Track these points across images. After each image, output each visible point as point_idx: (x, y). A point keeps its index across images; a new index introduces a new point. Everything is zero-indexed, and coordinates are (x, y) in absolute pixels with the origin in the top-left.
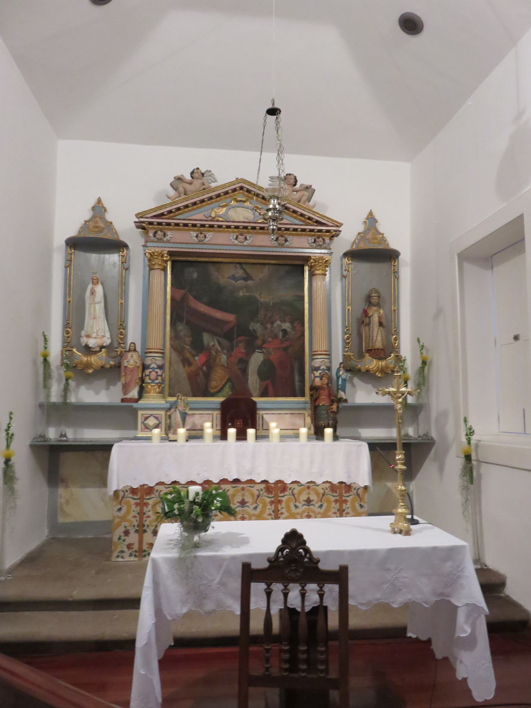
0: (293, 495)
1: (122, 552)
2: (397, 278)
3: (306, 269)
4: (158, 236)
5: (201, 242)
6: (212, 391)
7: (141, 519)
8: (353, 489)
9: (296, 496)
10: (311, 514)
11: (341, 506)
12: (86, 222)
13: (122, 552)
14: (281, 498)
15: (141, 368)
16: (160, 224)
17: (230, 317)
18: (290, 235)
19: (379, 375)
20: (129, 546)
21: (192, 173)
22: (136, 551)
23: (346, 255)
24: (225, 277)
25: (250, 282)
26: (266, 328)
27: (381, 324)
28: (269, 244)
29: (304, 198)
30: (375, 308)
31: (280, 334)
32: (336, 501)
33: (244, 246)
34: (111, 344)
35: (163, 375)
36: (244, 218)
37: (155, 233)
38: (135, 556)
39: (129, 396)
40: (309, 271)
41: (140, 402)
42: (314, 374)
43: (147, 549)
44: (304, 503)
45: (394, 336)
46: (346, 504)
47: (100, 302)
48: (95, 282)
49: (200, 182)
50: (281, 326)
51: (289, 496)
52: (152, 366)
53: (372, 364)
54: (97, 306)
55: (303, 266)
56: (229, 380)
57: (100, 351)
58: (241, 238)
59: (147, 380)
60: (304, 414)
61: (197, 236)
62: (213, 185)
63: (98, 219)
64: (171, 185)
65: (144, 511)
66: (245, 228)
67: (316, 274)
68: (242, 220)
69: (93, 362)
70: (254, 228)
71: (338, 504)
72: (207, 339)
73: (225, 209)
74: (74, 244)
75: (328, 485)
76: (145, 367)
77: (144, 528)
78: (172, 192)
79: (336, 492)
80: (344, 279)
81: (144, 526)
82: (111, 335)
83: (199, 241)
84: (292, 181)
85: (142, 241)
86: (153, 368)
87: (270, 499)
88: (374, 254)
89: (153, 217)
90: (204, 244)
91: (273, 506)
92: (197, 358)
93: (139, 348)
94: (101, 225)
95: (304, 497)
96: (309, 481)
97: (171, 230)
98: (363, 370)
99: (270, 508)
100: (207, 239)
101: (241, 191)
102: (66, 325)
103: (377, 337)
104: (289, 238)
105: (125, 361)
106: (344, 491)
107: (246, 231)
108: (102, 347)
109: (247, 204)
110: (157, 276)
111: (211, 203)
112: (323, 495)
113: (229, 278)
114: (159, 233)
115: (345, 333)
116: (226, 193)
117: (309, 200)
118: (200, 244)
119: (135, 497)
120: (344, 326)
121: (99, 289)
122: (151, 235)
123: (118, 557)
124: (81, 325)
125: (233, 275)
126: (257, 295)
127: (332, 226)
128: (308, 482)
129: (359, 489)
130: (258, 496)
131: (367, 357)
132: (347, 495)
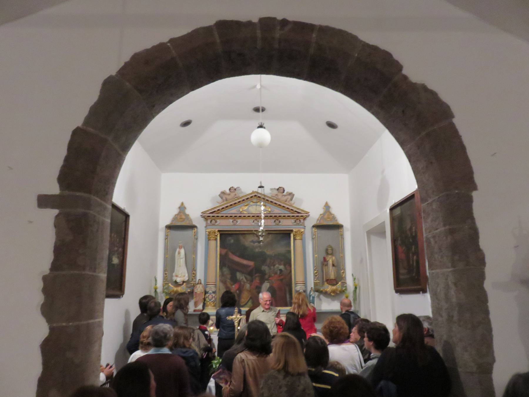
3: (292, 235)
5: (235, 225)
6: (242, 304)
15: (204, 293)
17: (251, 263)
21: (230, 189)
23: (313, 226)
24: (248, 241)
26: (270, 269)
27: (333, 265)
29: (288, 200)
30: (330, 256)
31: (279, 272)
34: (188, 280)
37: (211, 221)
40: (294, 235)
48: (180, 248)
49: (234, 194)
50: (278, 267)
53: (329, 288)
55: (289, 234)
56: (251, 298)
57: (183, 284)
59: (207, 299)
62: (241, 195)
72: (239, 276)
74: (169, 227)
76: (206, 293)
78: (220, 200)
82: (188, 275)
84: (282, 191)
85: (204, 223)
88: (329, 226)
92: (233, 286)
93: (203, 282)
94: (183, 217)
98: (324, 291)
102: (165, 270)
108: (184, 282)
110: (213, 243)
114: (213, 221)
115: (315, 270)
116: (248, 199)
117: (291, 200)
120: (314, 266)
121: (182, 251)
122: (209, 222)
124: (173, 270)
126: (265, 251)
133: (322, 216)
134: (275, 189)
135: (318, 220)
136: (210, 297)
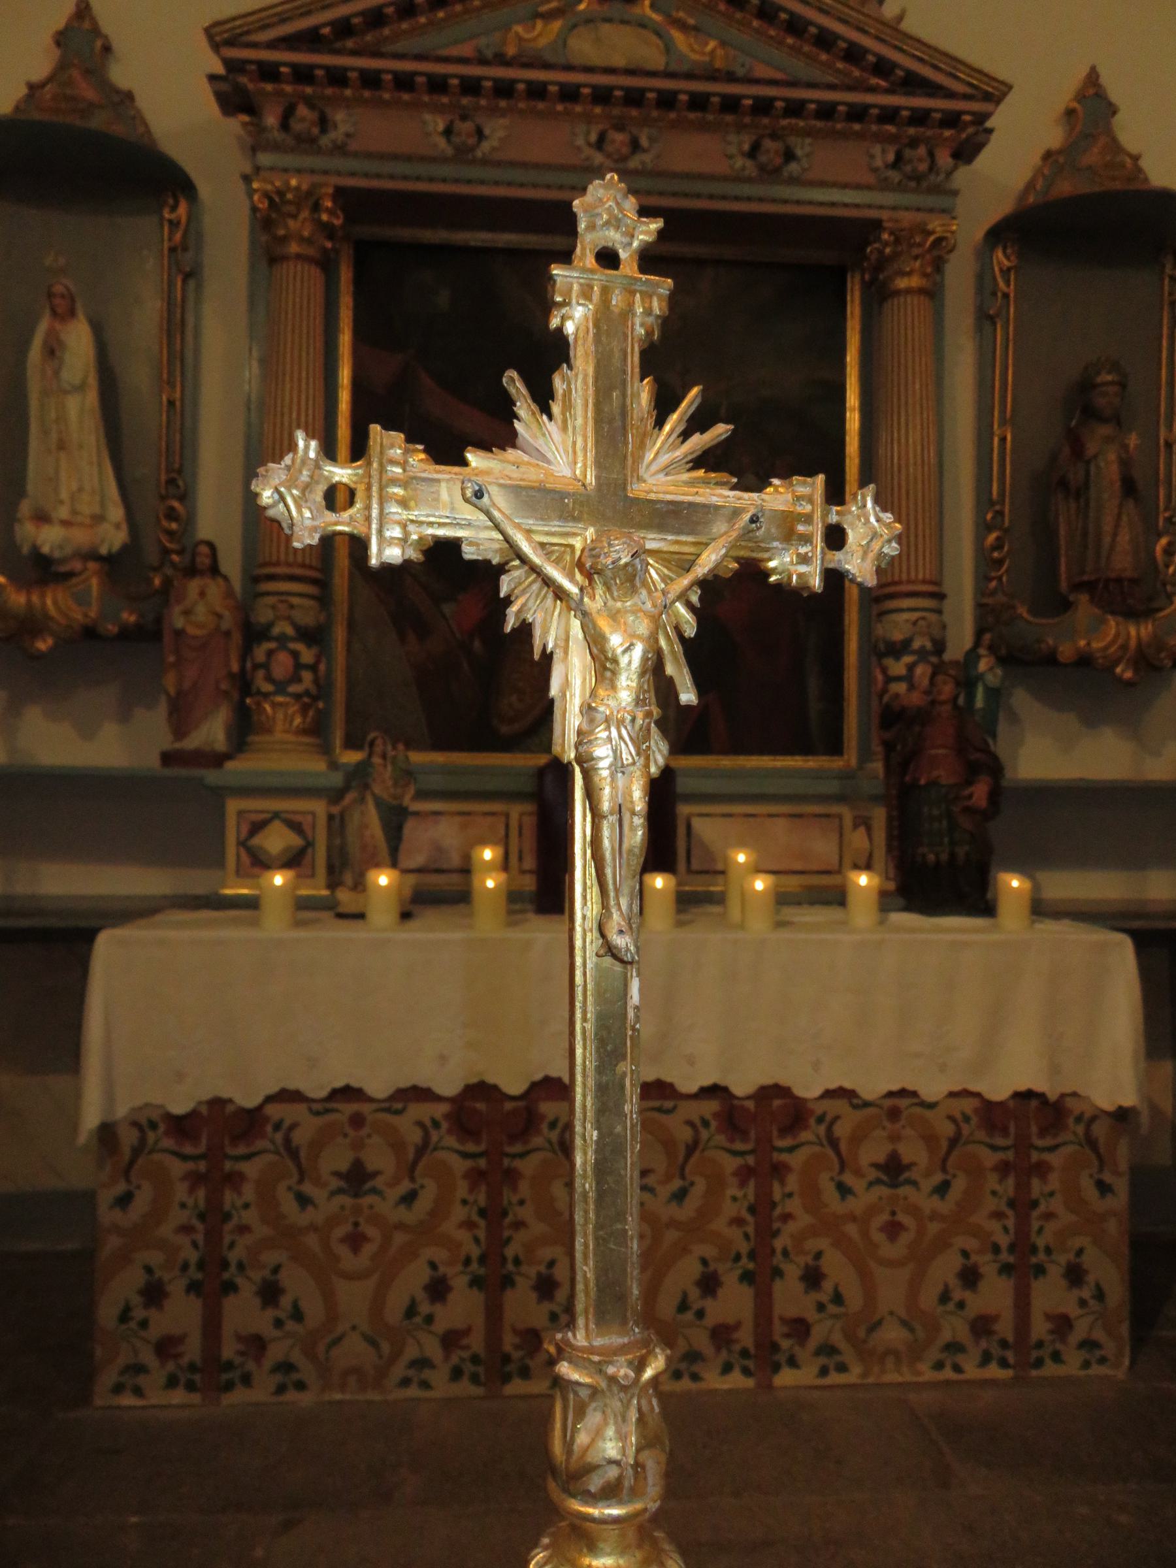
0: (833, 1143)
1: (139, 1369)
4: (297, 126)
5: (463, 154)
6: (505, 729)
7: (213, 1236)
8: (1071, 1121)
9: (843, 1146)
10: (901, 1217)
11: (1022, 1186)
12: (32, 87)
13: (139, 1369)
14: (784, 1157)
15: (237, 638)
16: (302, 75)
18: (808, 133)
19: (1128, 675)
20: (166, 1347)
22: (192, 1368)
23: (997, 235)
27: (1129, 487)
30: (1104, 430)
32: (1004, 1169)
34: (131, 549)
35: (322, 667)
38: (191, 1387)
39: (193, 742)
40: (866, 286)
41: (230, 765)
42: (884, 670)
43: (238, 1360)
44: (873, 1174)
45: (1164, 541)
46: (1043, 1177)
47: (81, 388)
51: (817, 1149)
52: (276, 630)
54: (73, 404)
58: (619, 138)
60: (840, 817)
61: (448, 132)
63: (75, 73)
65: (227, 1206)
66: (634, 98)
67: (898, 293)
68: (619, 61)
69: (52, 611)
70: (667, 101)
71: (1011, 1181)
73: (557, 25)
75: (968, 1105)
76: (253, 634)
77: (226, 1276)
79: (1005, 1132)
81: (225, 1265)
86: (282, 639)
87: (739, 1161)
89: (272, 45)
90: (473, 162)
91: (751, 1189)
92: (448, 609)
93: (231, 564)
94: (88, 92)
95: (873, 1152)
96: (895, 1087)
98: (1066, 652)
99: (739, 1194)
100: (486, 146)
103: (1115, 535)
105: (177, 610)
106: (1034, 1129)
107: (634, 113)
112: (954, 1142)
114: (302, 111)
115: (983, 527)
119: (188, 1150)
120: (983, 500)
121: (79, 340)
122: (271, 120)
123: (118, 1389)
127: (966, 97)
128: (890, 1094)
129: (1094, 1119)
130: (691, 1148)
131: (1084, 608)
132: (1048, 1142)
136: (282, 664)
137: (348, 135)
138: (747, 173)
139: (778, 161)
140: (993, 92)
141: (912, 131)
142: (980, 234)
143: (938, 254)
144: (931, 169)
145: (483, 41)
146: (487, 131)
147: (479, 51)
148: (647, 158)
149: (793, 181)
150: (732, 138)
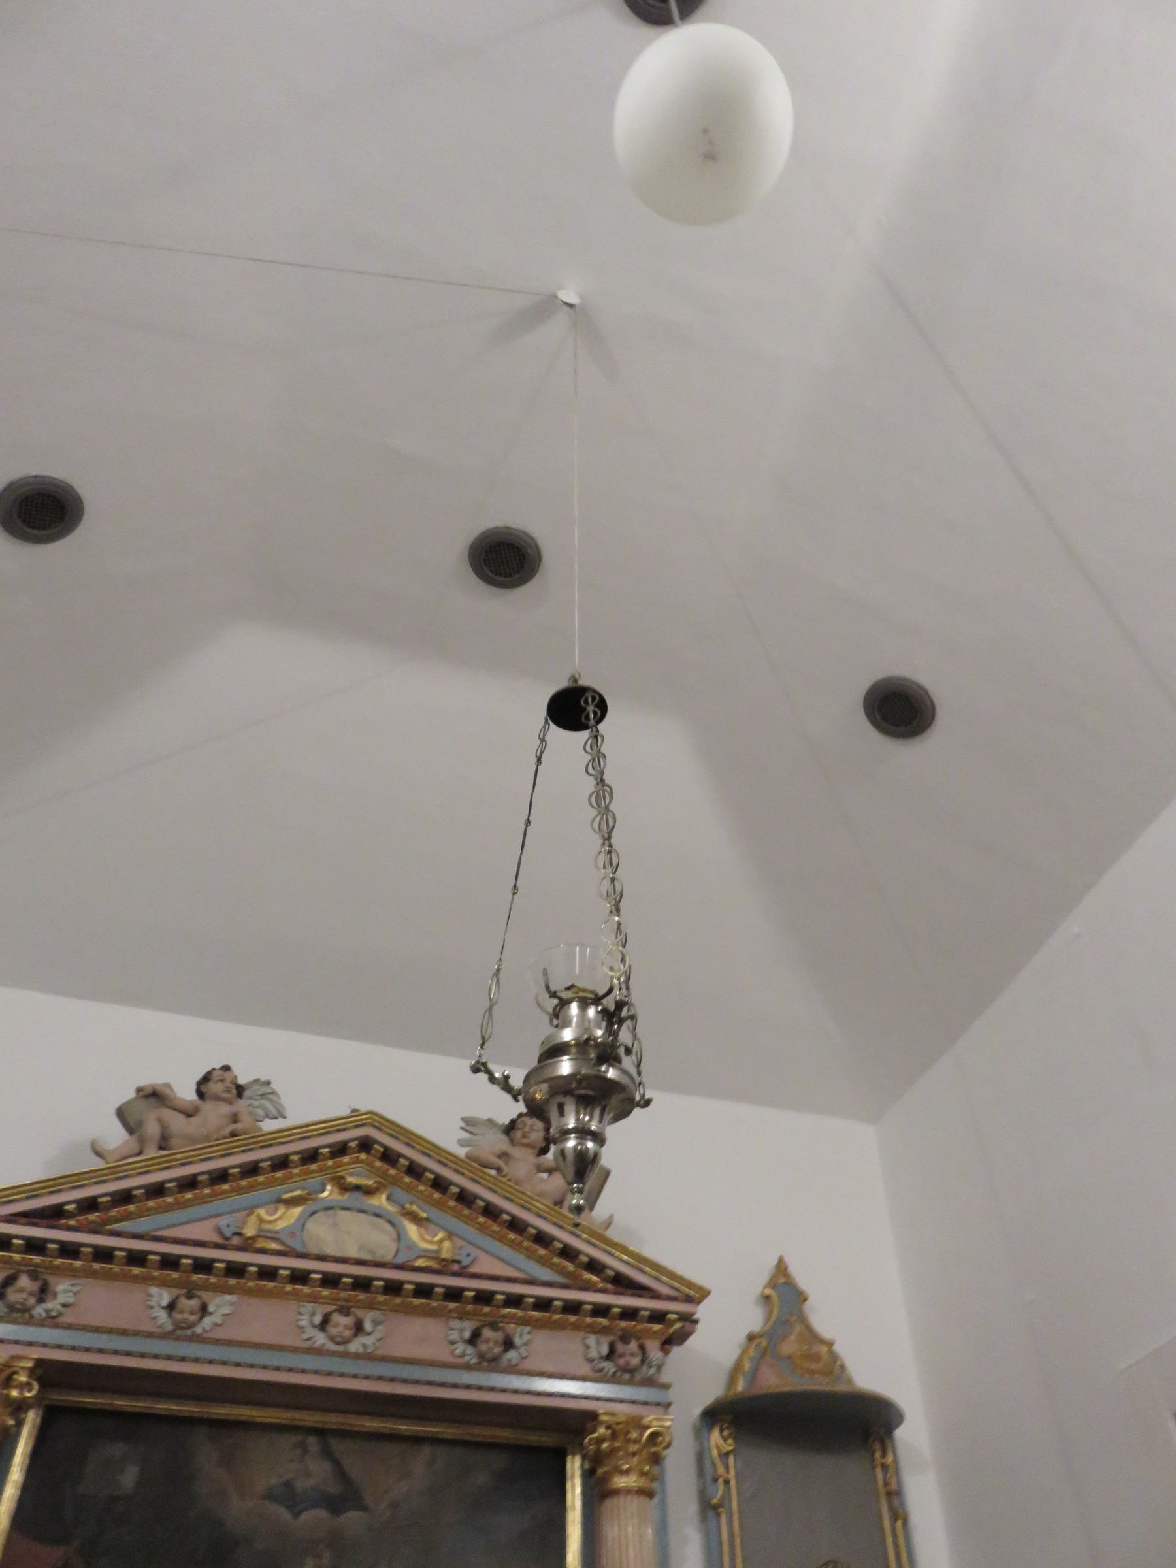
2: (899, 1515)
3: (574, 1466)
5: (181, 1331)
16: (34, 1246)
18: (524, 1322)
21: (206, 1079)
23: (712, 1416)
25: (352, 1519)
28: (444, 1355)
33: (345, 1355)
36: (361, 1248)
40: (588, 1475)
49: (225, 1109)
55: (559, 1457)
58: (341, 1323)
61: (171, 1307)
62: (268, 1126)
64: (121, 1114)
66: (362, 1284)
67: (616, 1492)
68: (353, 1253)
70: (394, 1288)
73: (297, 1211)
78: (115, 1136)
80: (711, 1513)
83: (178, 1326)
97: (74, 1273)
100: (207, 1322)
101: (363, 1156)
104: (521, 1334)
107: (362, 1296)
109: (380, 1201)
111: (251, 1188)
113: (270, 1496)
116: (311, 1156)
118: (178, 1339)
125: (288, 1485)
133: (763, 1346)
134: (490, 1122)
135: (737, 1367)
137: (64, 1305)
138: (467, 1358)
139: (497, 1350)
140: (696, 1295)
141: (623, 1324)
142: (697, 1411)
143: (654, 1450)
144: (643, 1361)
145: (223, 1222)
146: (211, 1308)
147: (220, 1232)
148: (368, 1340)
149: (514, 1370)
150: (456, 1324)
